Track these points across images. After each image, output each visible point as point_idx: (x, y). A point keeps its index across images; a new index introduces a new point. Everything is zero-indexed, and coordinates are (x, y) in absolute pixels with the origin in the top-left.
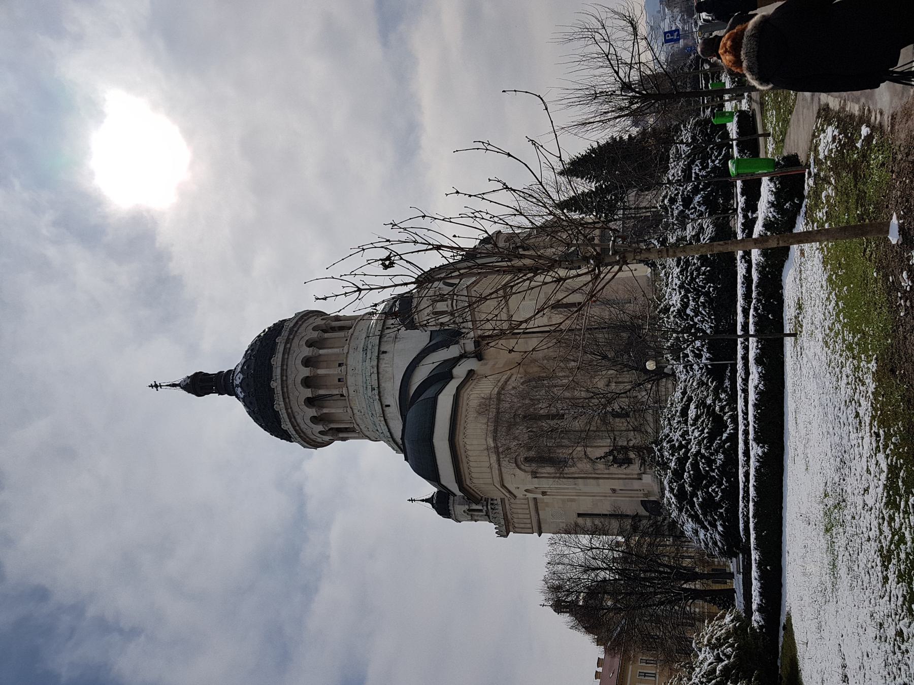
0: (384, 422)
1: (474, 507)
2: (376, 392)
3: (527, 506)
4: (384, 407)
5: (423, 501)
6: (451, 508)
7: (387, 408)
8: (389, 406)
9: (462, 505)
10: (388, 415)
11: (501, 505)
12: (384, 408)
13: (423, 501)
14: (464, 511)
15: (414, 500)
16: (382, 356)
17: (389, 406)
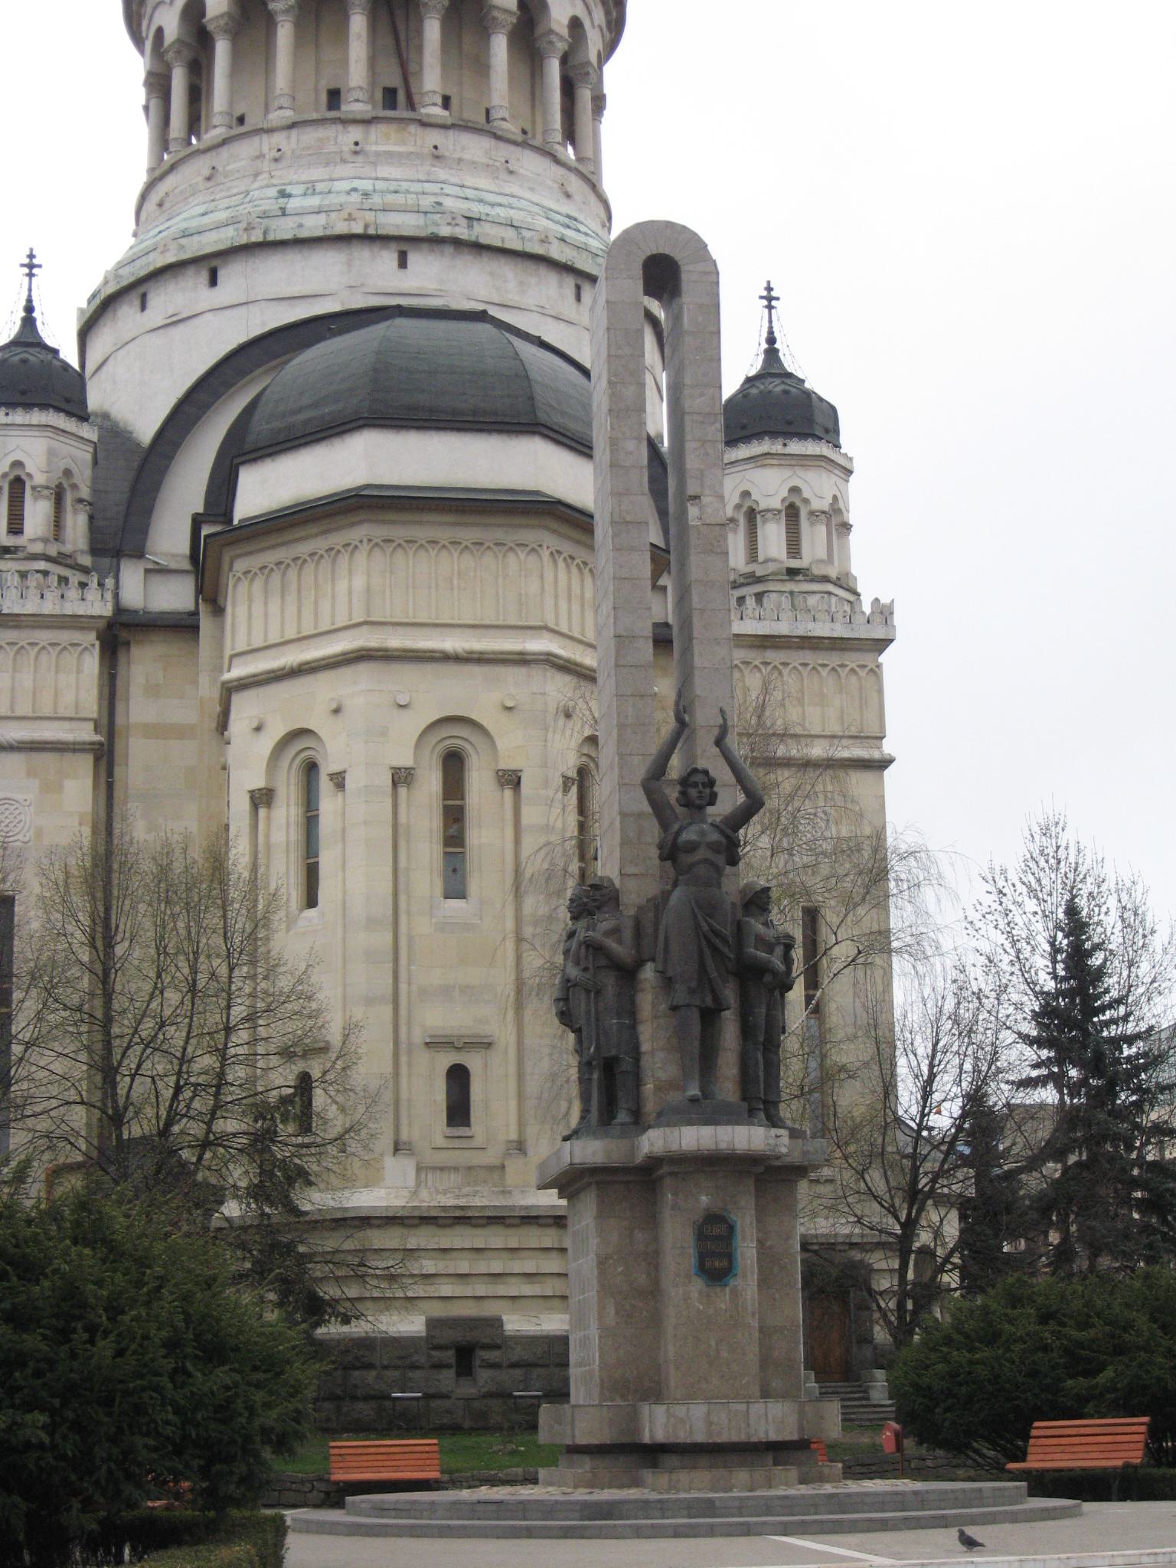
0: (341, 228)
1: (37, 514)
2: (462, 232)
3: (47, 711)
4: (404, 246)
5: (29, 309)
6: (37, 417)
7: (395, 256)
8: (403, 263)
9: (49, 463)
10: (362, 254)
11: (57, 611)
12: (394, 246)
13: (29, 309)
14: (18, 464)
15: (31, 275)
16: (570, 282)
17: (403, 263)
